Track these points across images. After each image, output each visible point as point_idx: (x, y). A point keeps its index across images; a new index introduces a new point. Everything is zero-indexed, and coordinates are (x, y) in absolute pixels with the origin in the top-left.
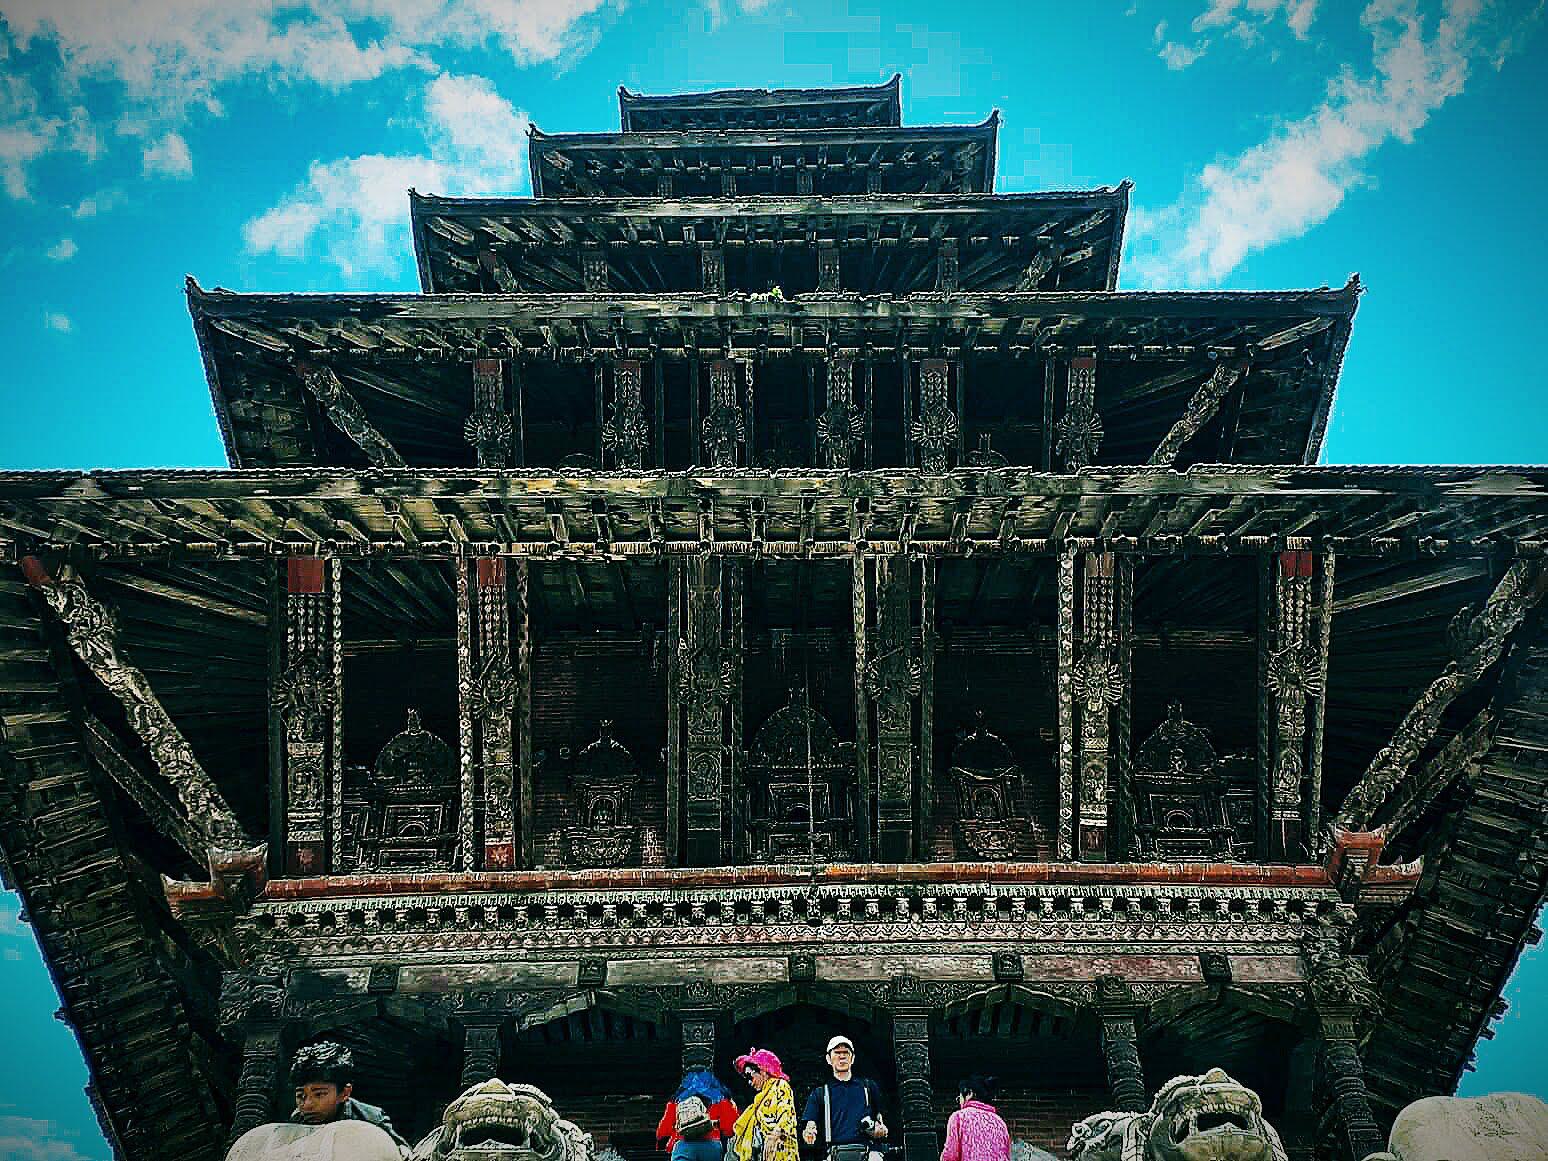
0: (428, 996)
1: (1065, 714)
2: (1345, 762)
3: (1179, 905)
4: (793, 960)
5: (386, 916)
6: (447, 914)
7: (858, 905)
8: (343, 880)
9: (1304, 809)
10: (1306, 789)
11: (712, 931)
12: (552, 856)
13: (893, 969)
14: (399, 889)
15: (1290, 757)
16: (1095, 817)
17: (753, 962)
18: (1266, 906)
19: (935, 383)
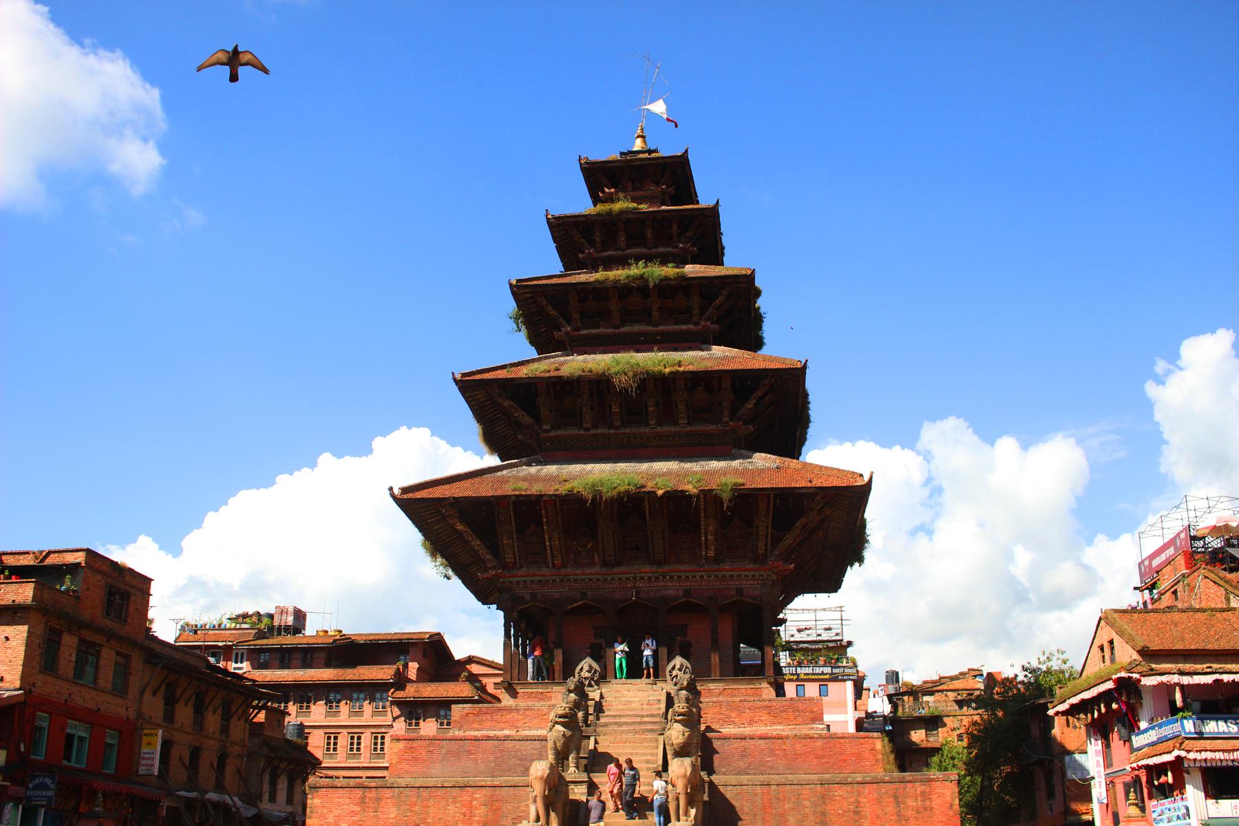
7: (650, 578)
8: (520, 573)
14: (534, 575)
16: (711, 553)
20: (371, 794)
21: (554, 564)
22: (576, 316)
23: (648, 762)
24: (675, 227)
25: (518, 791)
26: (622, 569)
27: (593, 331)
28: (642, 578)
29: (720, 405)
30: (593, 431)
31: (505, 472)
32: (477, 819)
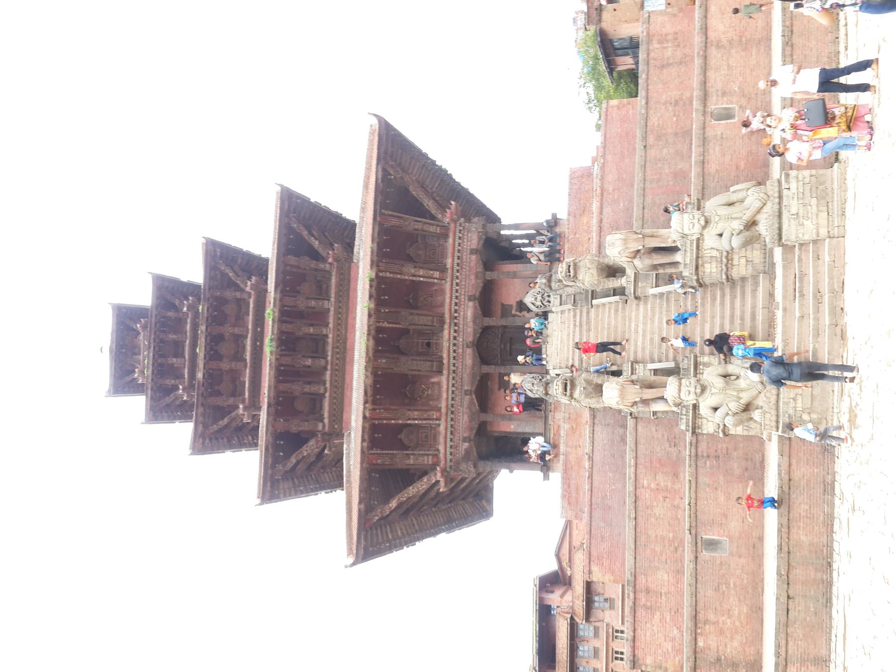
0: (471, 429)
1: (414, 278)
2: (423, 213)
3: (459, 258)
4: (468, 347)
5: (451, 440)
6: (452, 426)
7: (455, 331)
9: (438, 226)
10: (433, 225)
11: (459, 365)
12: (436, 403)
13: (471, 324)
14: (446, 437)
15: (426, 227)
16: (437, 274)
17: (467, 357)
18: (460, 238)
19: (289, 301)
20: (643, 599)
21: (437, 419)
22: (231, 401)
23: (617, 311)
24: (171, 314)
25: (642, 440)
26: (445, 356)
27: (247, 385)
28: (455, 338)
29: (316, 270)
30: (328, 385)
31: (352, 463)
32: (670, 484)
